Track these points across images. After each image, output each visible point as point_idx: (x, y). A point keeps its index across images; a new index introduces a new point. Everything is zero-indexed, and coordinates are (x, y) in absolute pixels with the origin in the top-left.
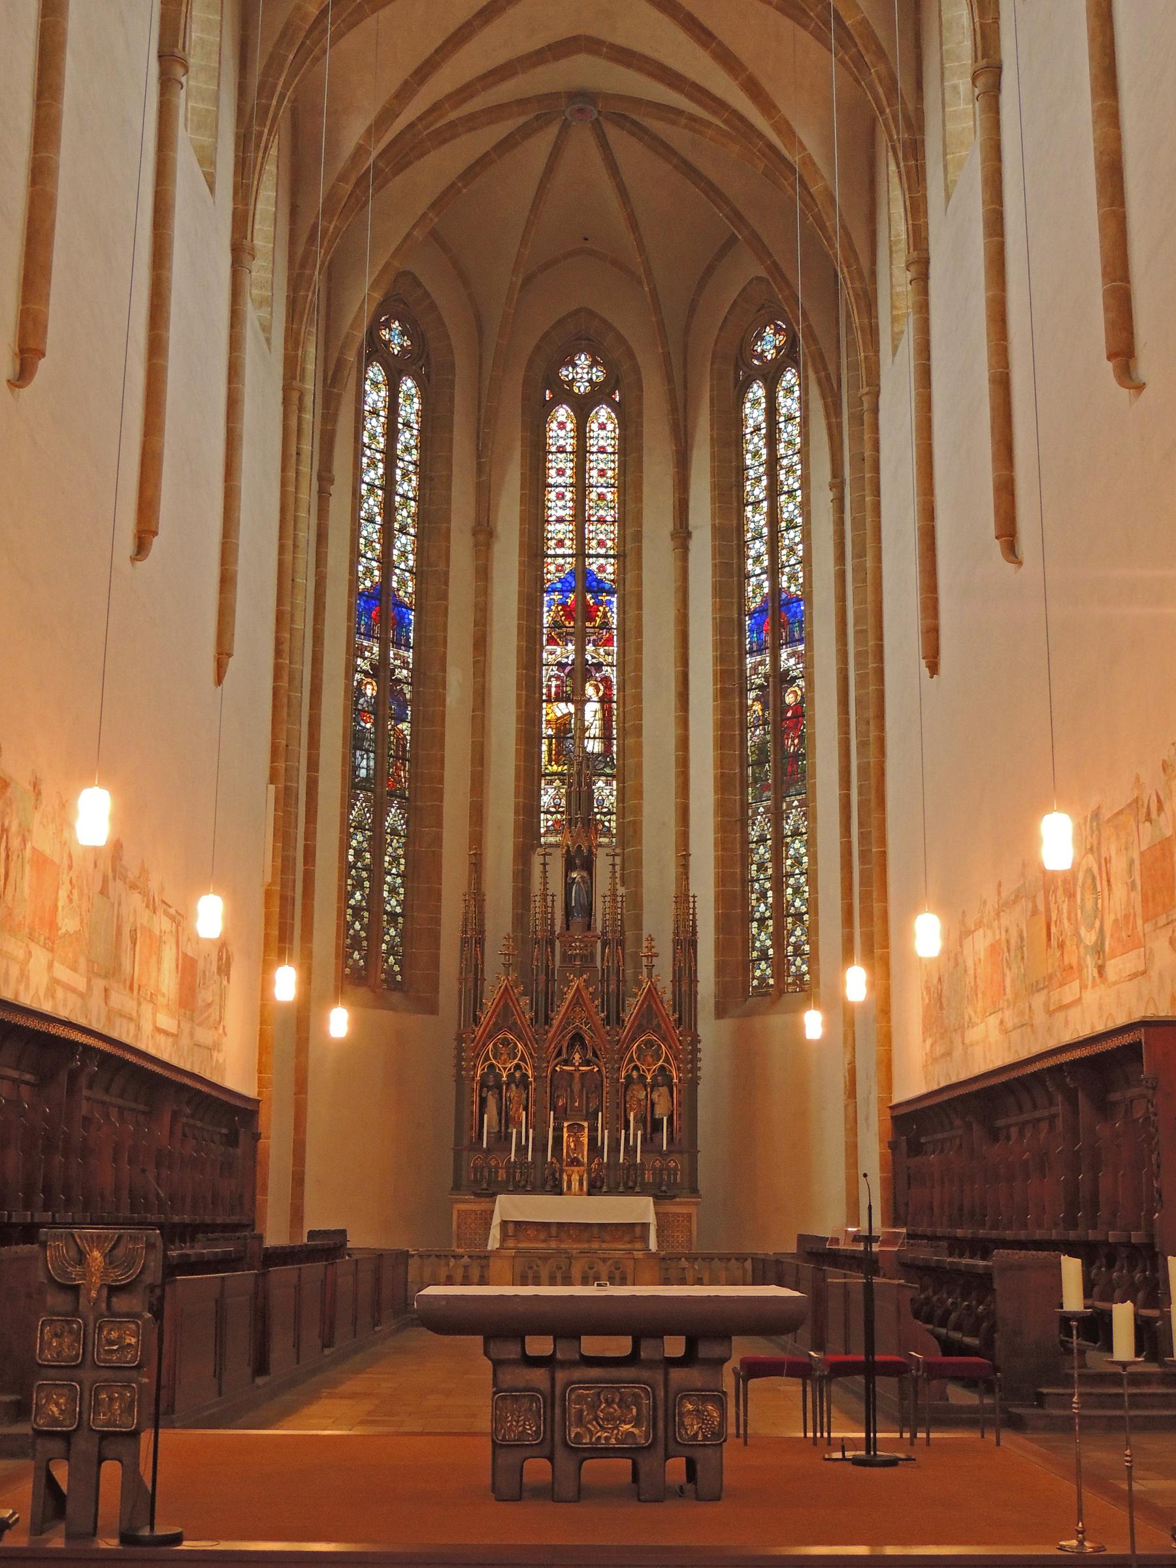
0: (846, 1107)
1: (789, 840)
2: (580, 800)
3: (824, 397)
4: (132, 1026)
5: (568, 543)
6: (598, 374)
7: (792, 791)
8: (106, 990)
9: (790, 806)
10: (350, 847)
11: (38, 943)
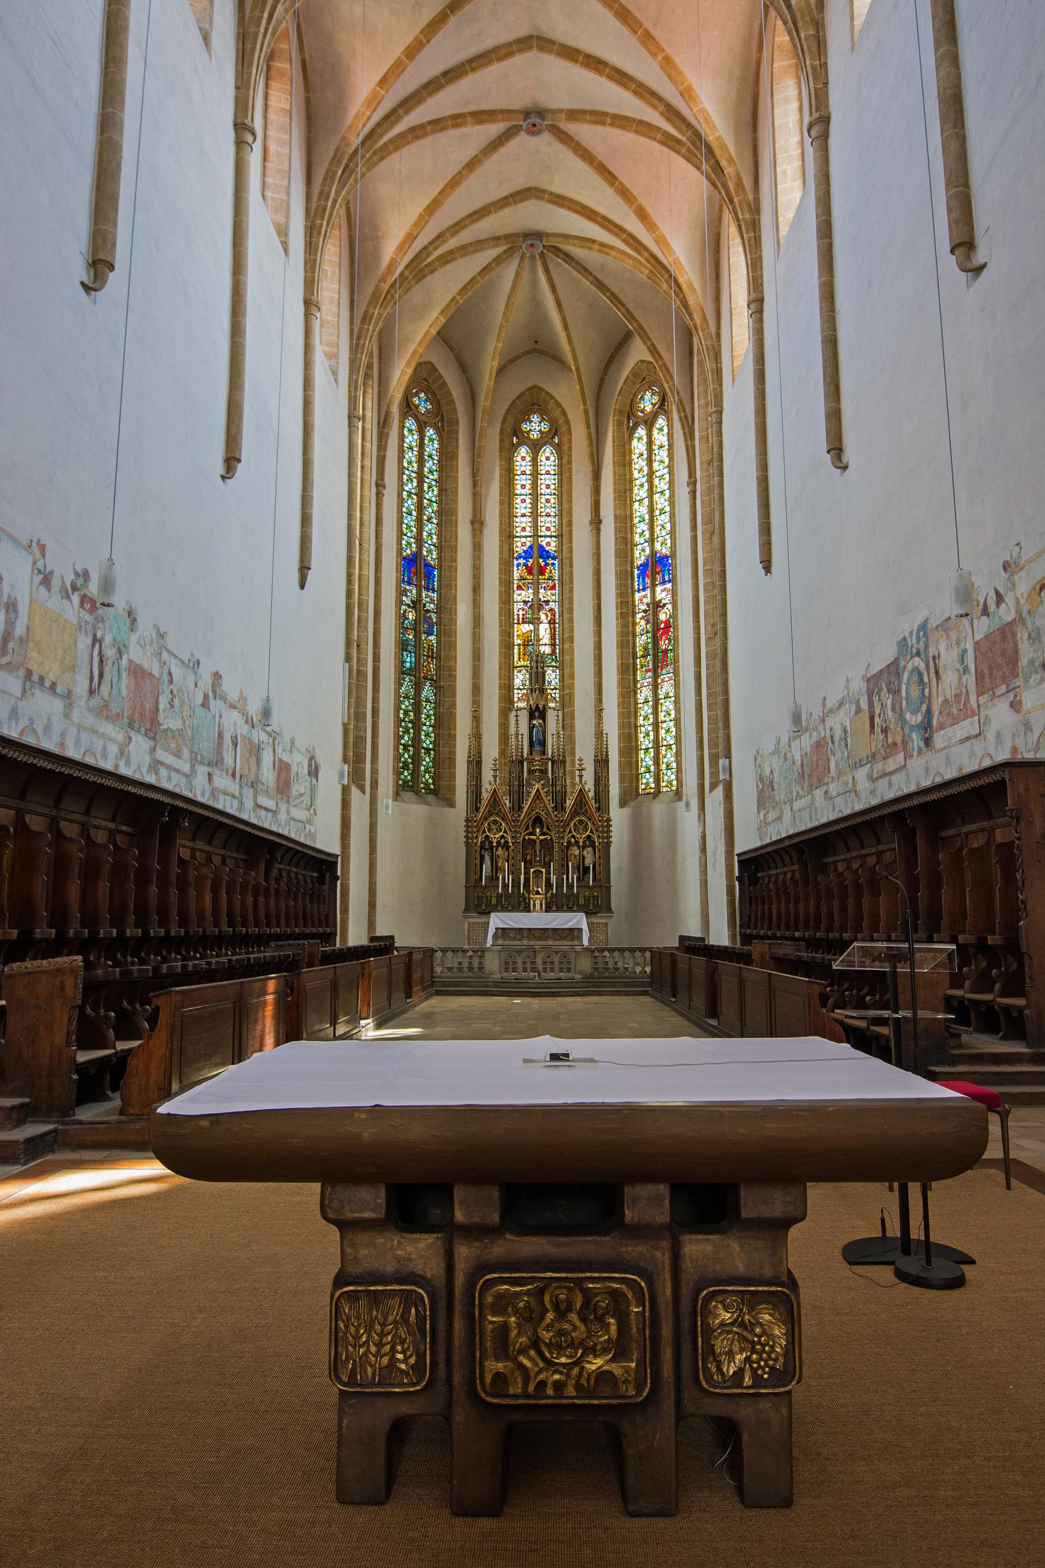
2: (537, 677)
3: (683, 429)
4: (235, 803)
5: (528, 529)
6: (545, 427)
7: (664, 672)
8: (209, 774)
9: (663, 681)
11: (139, 732)
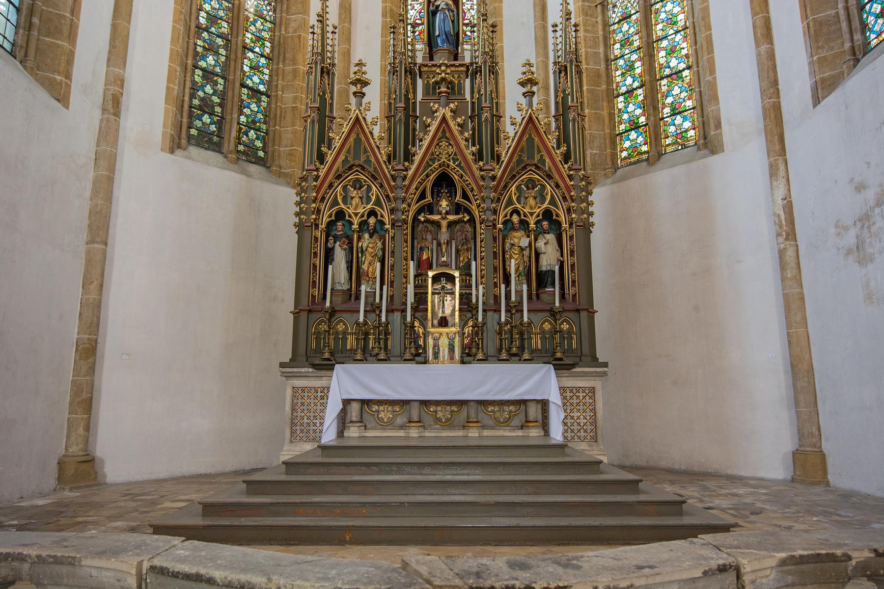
0: (781, 253)
1: (658, 6)
10: (201, 9)
